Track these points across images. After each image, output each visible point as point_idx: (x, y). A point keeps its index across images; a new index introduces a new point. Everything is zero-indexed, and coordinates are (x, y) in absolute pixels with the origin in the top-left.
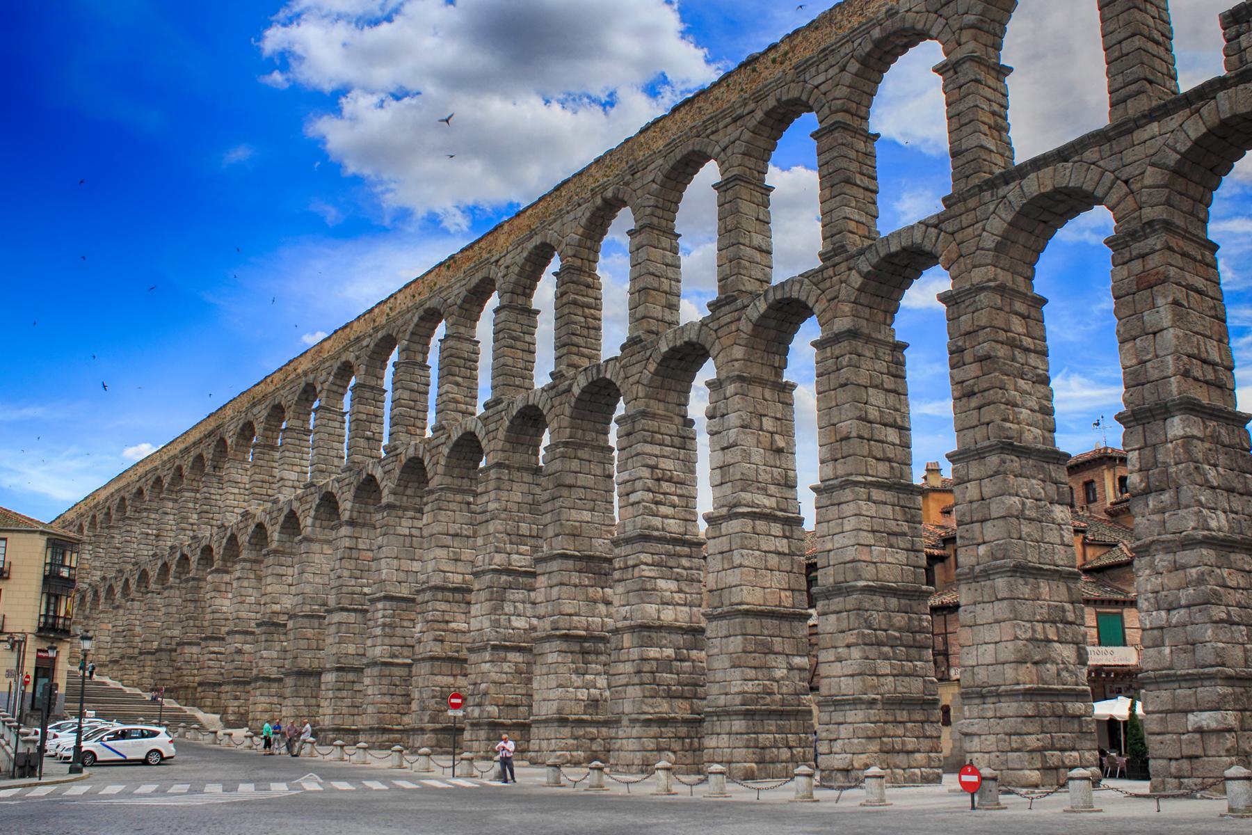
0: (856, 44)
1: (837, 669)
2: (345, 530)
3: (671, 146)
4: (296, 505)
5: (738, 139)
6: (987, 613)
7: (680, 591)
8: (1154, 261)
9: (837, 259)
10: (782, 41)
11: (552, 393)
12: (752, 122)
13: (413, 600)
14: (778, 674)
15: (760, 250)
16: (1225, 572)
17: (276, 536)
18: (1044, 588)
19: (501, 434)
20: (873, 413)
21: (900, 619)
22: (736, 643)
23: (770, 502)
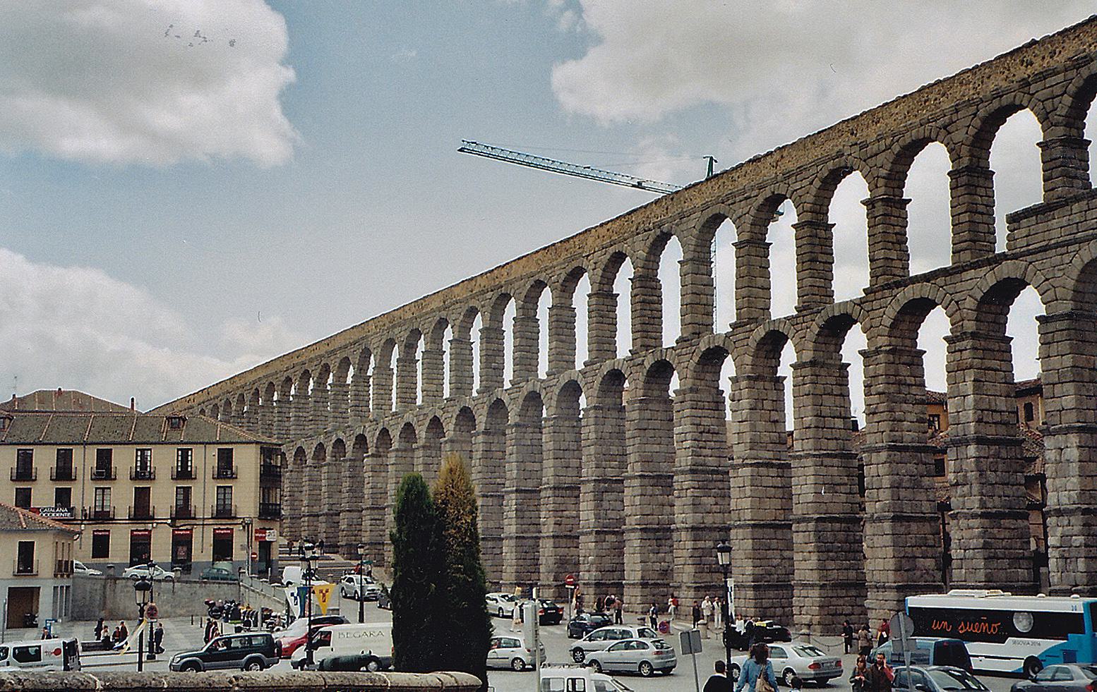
0: (819, 168)
1: (804, 565)
2: (480, 438)
3: (706, 207)
4: (439, 413)
5: (748, 213)
6: (879, 541)
7: (716, 504)
8: (966, 354)
9: (805, 313)
10: (775, 151)
11: (631, 363)
12: (756, 204)
13: (535, 491)
14: (775, 562)
15: (763, 288)
16: (996, 531)
17: (423, 435)
18: (914, 527)
19: (596, 385)
20: (826, 411)
21: (841, 536)
22: (749, 544)
23: (769, 455)
